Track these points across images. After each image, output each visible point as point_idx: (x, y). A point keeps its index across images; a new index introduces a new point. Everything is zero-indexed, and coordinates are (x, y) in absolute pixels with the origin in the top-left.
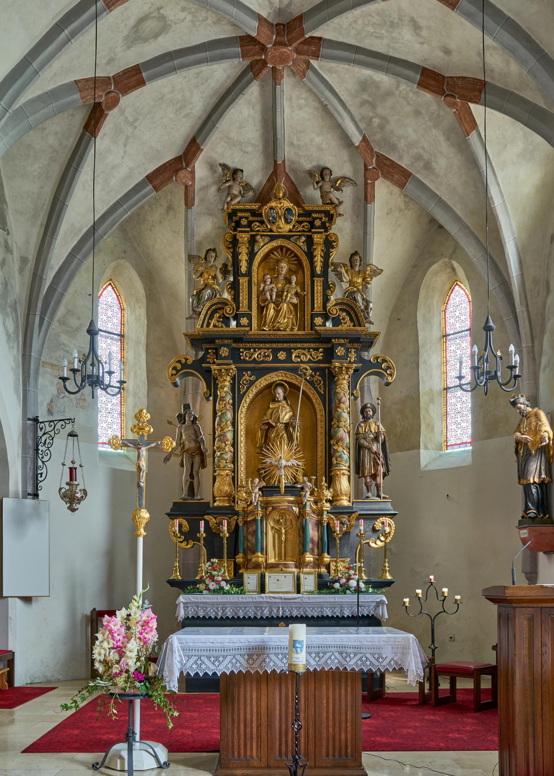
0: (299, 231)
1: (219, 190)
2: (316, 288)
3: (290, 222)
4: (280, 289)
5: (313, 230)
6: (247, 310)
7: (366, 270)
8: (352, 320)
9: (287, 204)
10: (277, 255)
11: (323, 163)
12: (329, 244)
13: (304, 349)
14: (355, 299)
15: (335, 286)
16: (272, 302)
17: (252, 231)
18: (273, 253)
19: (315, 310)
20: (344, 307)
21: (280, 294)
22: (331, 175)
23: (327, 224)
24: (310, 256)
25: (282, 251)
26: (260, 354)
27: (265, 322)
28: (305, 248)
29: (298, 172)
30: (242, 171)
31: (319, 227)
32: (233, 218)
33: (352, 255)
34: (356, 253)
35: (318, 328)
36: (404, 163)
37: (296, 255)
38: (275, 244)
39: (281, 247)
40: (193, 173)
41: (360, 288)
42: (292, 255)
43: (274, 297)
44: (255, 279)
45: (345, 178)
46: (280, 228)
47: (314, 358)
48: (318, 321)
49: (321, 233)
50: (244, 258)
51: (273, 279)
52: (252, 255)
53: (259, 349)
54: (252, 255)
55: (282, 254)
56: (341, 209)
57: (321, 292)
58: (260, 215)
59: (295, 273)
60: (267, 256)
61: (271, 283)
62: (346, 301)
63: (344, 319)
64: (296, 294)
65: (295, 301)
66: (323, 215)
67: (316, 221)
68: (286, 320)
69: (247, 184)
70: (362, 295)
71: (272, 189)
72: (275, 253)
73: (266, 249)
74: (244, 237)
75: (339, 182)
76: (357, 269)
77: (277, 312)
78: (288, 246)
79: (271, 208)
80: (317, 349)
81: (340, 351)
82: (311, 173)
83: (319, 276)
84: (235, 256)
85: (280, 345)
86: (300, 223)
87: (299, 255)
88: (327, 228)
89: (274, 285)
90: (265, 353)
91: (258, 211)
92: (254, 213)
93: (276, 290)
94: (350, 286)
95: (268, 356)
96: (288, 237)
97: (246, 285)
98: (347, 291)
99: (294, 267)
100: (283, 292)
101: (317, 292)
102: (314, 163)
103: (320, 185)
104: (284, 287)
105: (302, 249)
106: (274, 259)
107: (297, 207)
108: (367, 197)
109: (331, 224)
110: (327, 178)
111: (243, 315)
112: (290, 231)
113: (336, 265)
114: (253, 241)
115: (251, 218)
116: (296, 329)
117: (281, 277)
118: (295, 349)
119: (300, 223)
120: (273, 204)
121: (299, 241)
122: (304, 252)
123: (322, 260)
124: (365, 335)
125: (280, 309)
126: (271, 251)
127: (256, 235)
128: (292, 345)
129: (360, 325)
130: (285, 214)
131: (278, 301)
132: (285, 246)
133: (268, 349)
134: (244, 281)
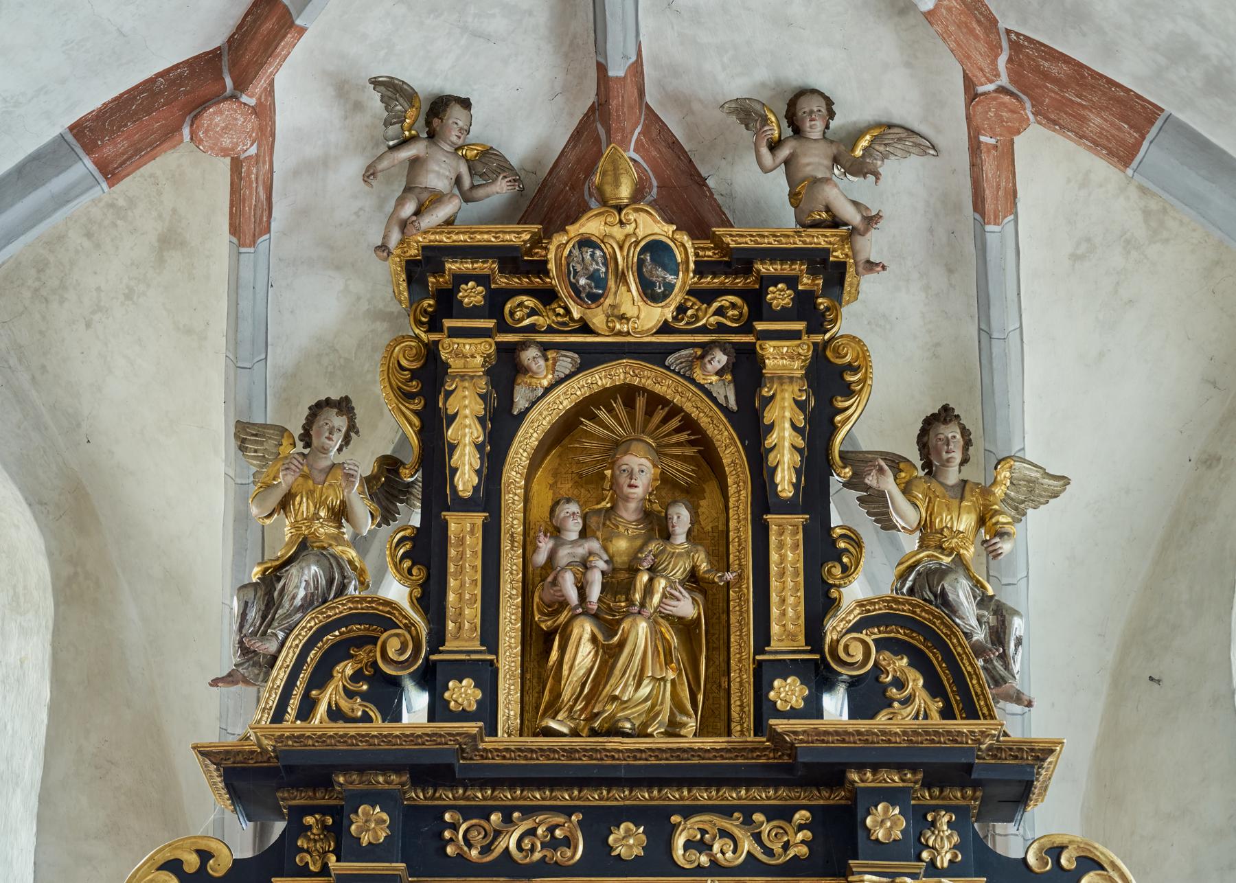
0: (704, 330)
1: (370, 174)
2: (774, 557)
3: (665, 296)
4: (620, 560)
5: (760, 326)
6: (476, 645)
7: (995, 482)
8: (934, 687)
9: (650, 225)
10: (610, 422)
11: (796, 76)
12: (831, 381)
13: (726, 811)
14: (943, 600)
15: (858, 544)
16: (586, 613)
17: (503, 327)
18: (593, 417)
19: (775, 645)
20: (901, 634)
21: (619, 582)
22: (831, 114)
23: (823, 302)
24: (751, 426)
25: (630, 404)
26: (532, 832)
27: (557, 695)
28: (727, 394)
29: (696, 106)
30: (466, 104)
31: (784, 315)
32: (428, 278)
33: (930, 423)
34: (945, 415)
35: (780, 725)
36: (1127, 71)
37: (689, 424)
38: (601, 378)
39: (628, 393)
40: (264, 113)
41: (969, 553)
42: (675, 423)
43: (595, 593)
44: (512, 521)
45: (890, 126)
46: (623, 318)
47: (769, 852)
48: (788, 692)
49: (795, 335)
50: (466, 435)
51: (593, 521)
52: (501, 424)
53: (528, 811)
54: (501, 424)
55: (632, 417)
56: (873, 246)
57: (796, 574)
58: (541, 268)
59: (690, 494)
60: (566, 429)
61: (583, 534)
62: (905, 611)
63: (900, 684)
64: (693, 580)
65: (686, 607)
66: (798, 268)
67: (778, 291)
68: (645, 690)
69: (487, 153)
70: (978, 584)
71: (590, 170)
72: (602, 414)
73: (564, 400)
74: (469, 355)
75: (864, 143)
76: (952, 476)
77: (609, 654)
78: (658, 389)
79: (586, 242)
80: (782, 813)
81: (885, 822)
82: (747, 113)
83: (787, 507)
84: (433, 425)
85: (620, 797)
86: (706, 296)
87: (704, 421)
88: (823, 315)
89: (594, 545)
90: (551, 830)
91: (529, 252)
92: (510, 259)
93: (602, 565)
94: (923, 546)
95: (568, 842)
96: (653, 354)
97: (474, 543)
98: (911, 568)
99: (681, 471)
100: (634, 571)
101: (782, 574)
102: (762, 74)
103: (784, 152)
104: (641, 550)
105: (714, 400)
106: (599, 439)
107: (693, 237)
108: (988, 195)
109: (839, 299)
110: (815, 129)
111: (460, 669)
112: (665, 328)
113: (859, 462)
114: (506, 370)
115: (502, 281)
116: (692, 724)
117: (629, 512)
118: (688, 812)
119: (706, 296)
120: (591, 226)
121: (703, 367)
122: (725, 409)
123: (800, 443)
124: (995, 751)
125: (621, 645)
126: (585, 409)
127: (524, 345)
128: (673, 796)
129: (972, 714)
130: (641, 263)
131: (611, 611)
132: (644, 390)
133: (568, 811)
134: (464, 529)
